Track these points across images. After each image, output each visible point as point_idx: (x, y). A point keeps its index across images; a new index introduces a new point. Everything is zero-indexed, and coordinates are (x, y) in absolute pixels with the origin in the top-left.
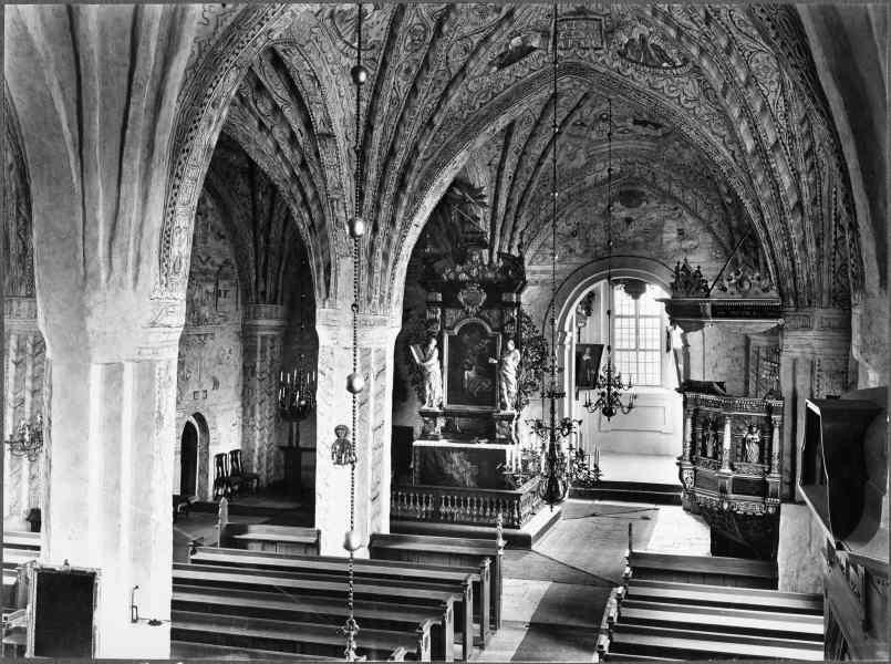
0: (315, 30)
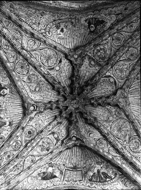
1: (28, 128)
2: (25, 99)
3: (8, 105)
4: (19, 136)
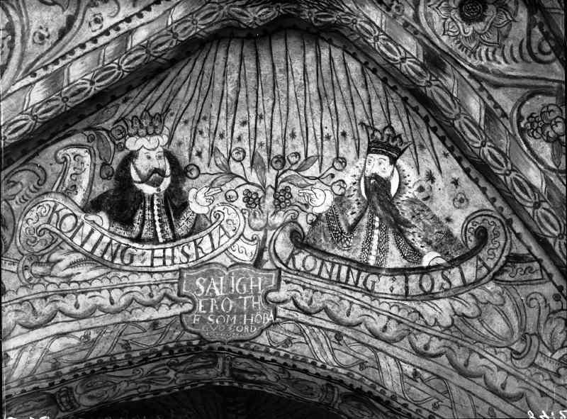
0: (283, 294)
1: (435, 14)
2: (210, 25)
3: (245, 137)
4: (490, 98)
